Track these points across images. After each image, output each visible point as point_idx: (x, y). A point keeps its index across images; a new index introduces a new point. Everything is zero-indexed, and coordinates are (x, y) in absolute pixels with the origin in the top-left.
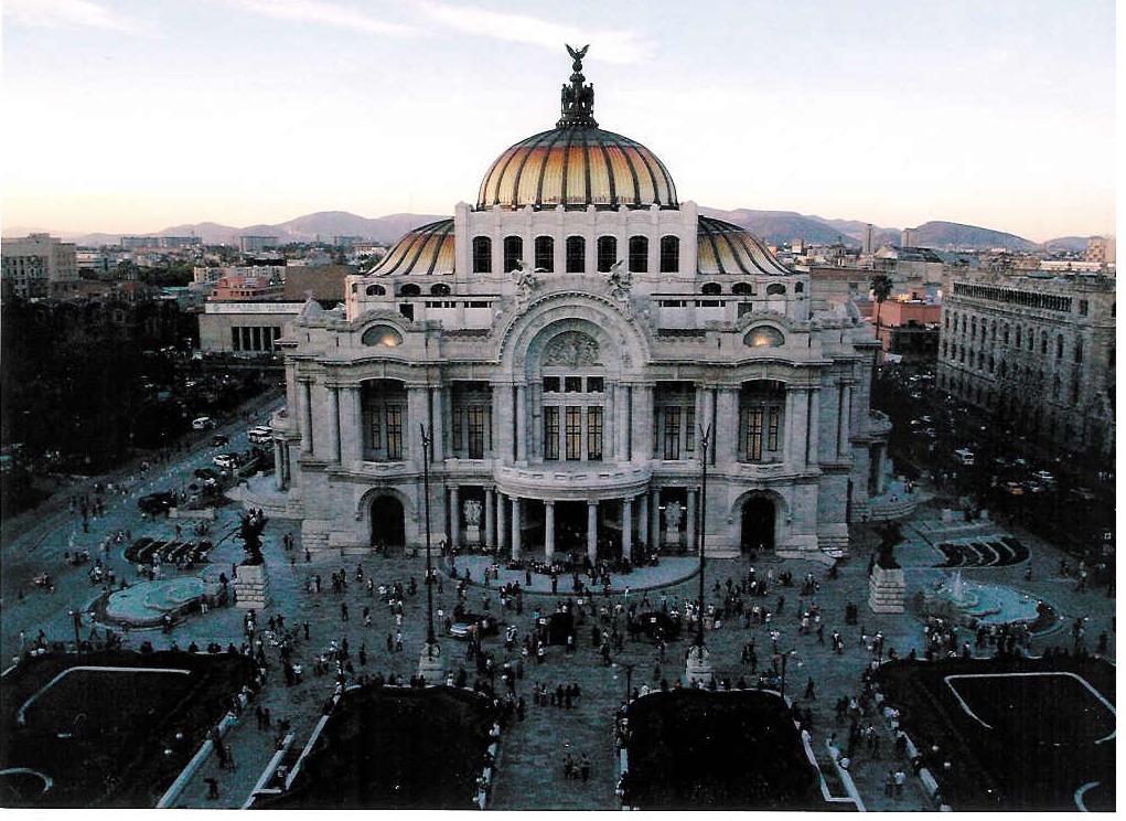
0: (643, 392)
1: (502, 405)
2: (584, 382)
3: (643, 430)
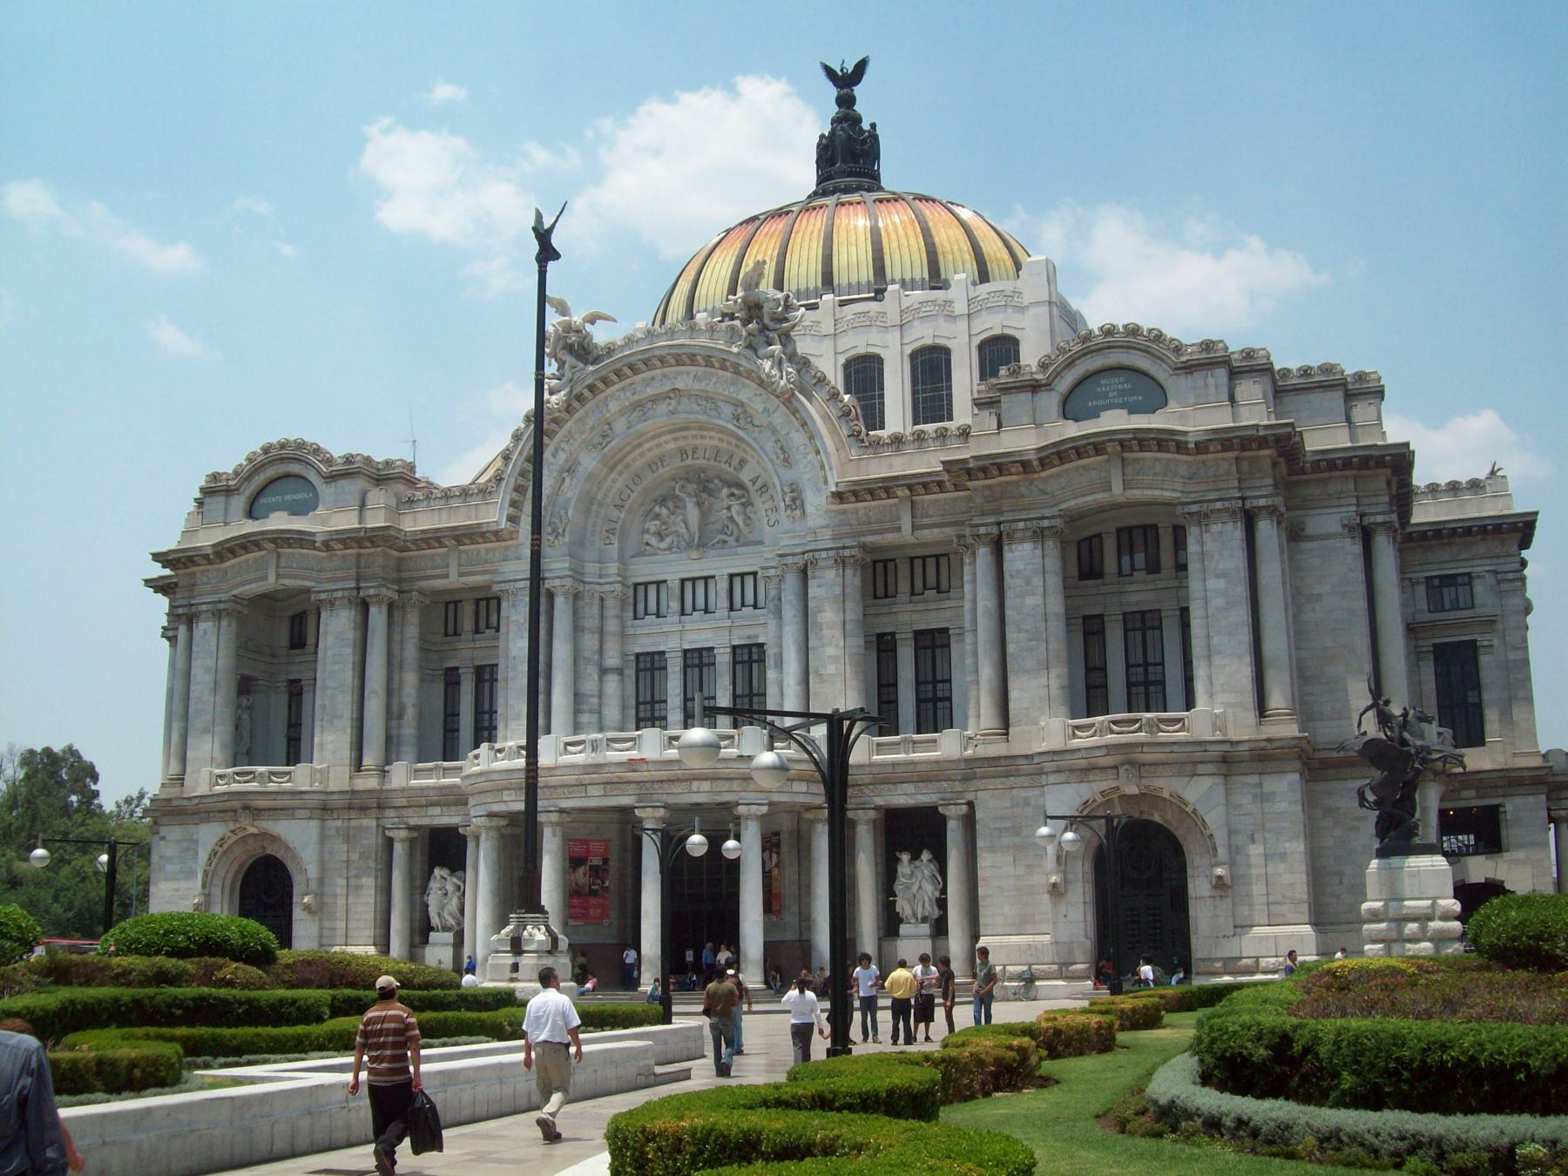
0: (831, 574)
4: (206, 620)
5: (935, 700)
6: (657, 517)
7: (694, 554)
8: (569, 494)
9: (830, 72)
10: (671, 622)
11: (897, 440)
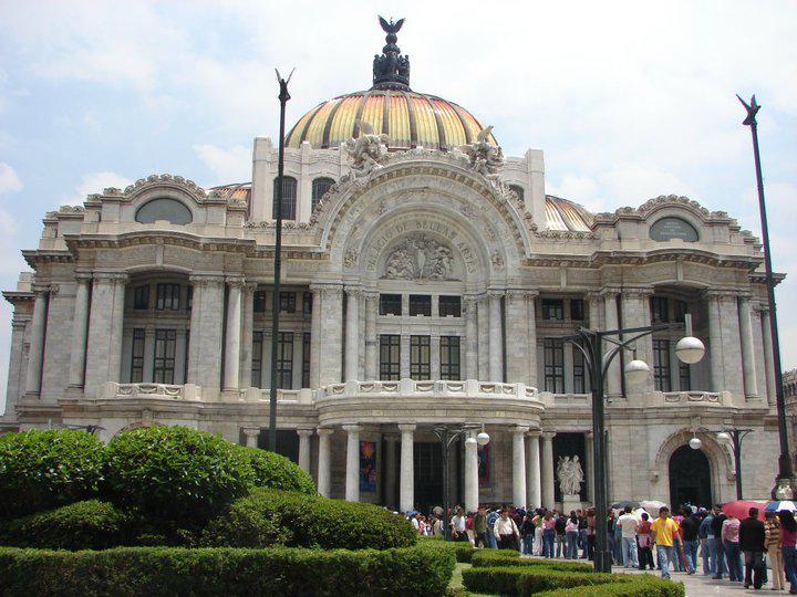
0: (521, 303)
1: (326, 318)
2: (435, 304)
3: (521, 355)
4: (105, 284)
5: (554, 376)
7: (421, 282)
9: (383, 22)
10: (405, 317)
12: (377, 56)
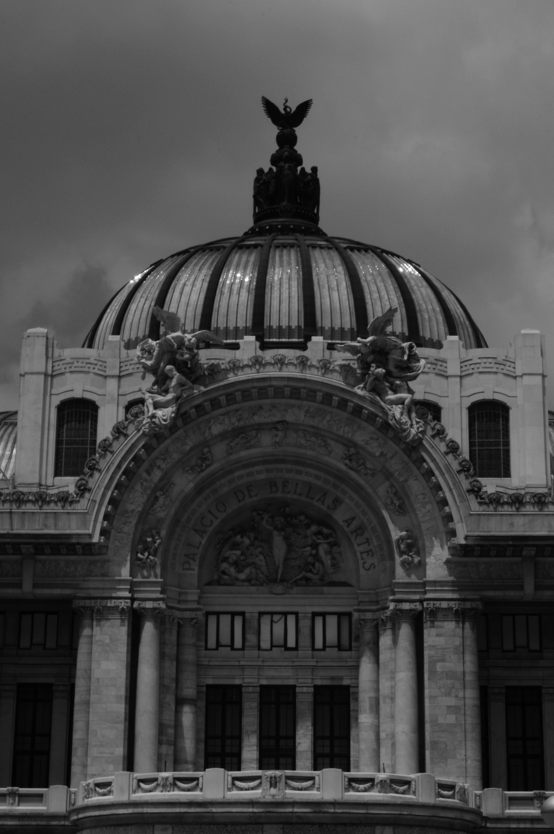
0: (450, 626)
6: (235, 546)
7: (279, 588)
8: (162, 515)
9: (270, 108)
11: (517, 501)
12: (260, 172)
